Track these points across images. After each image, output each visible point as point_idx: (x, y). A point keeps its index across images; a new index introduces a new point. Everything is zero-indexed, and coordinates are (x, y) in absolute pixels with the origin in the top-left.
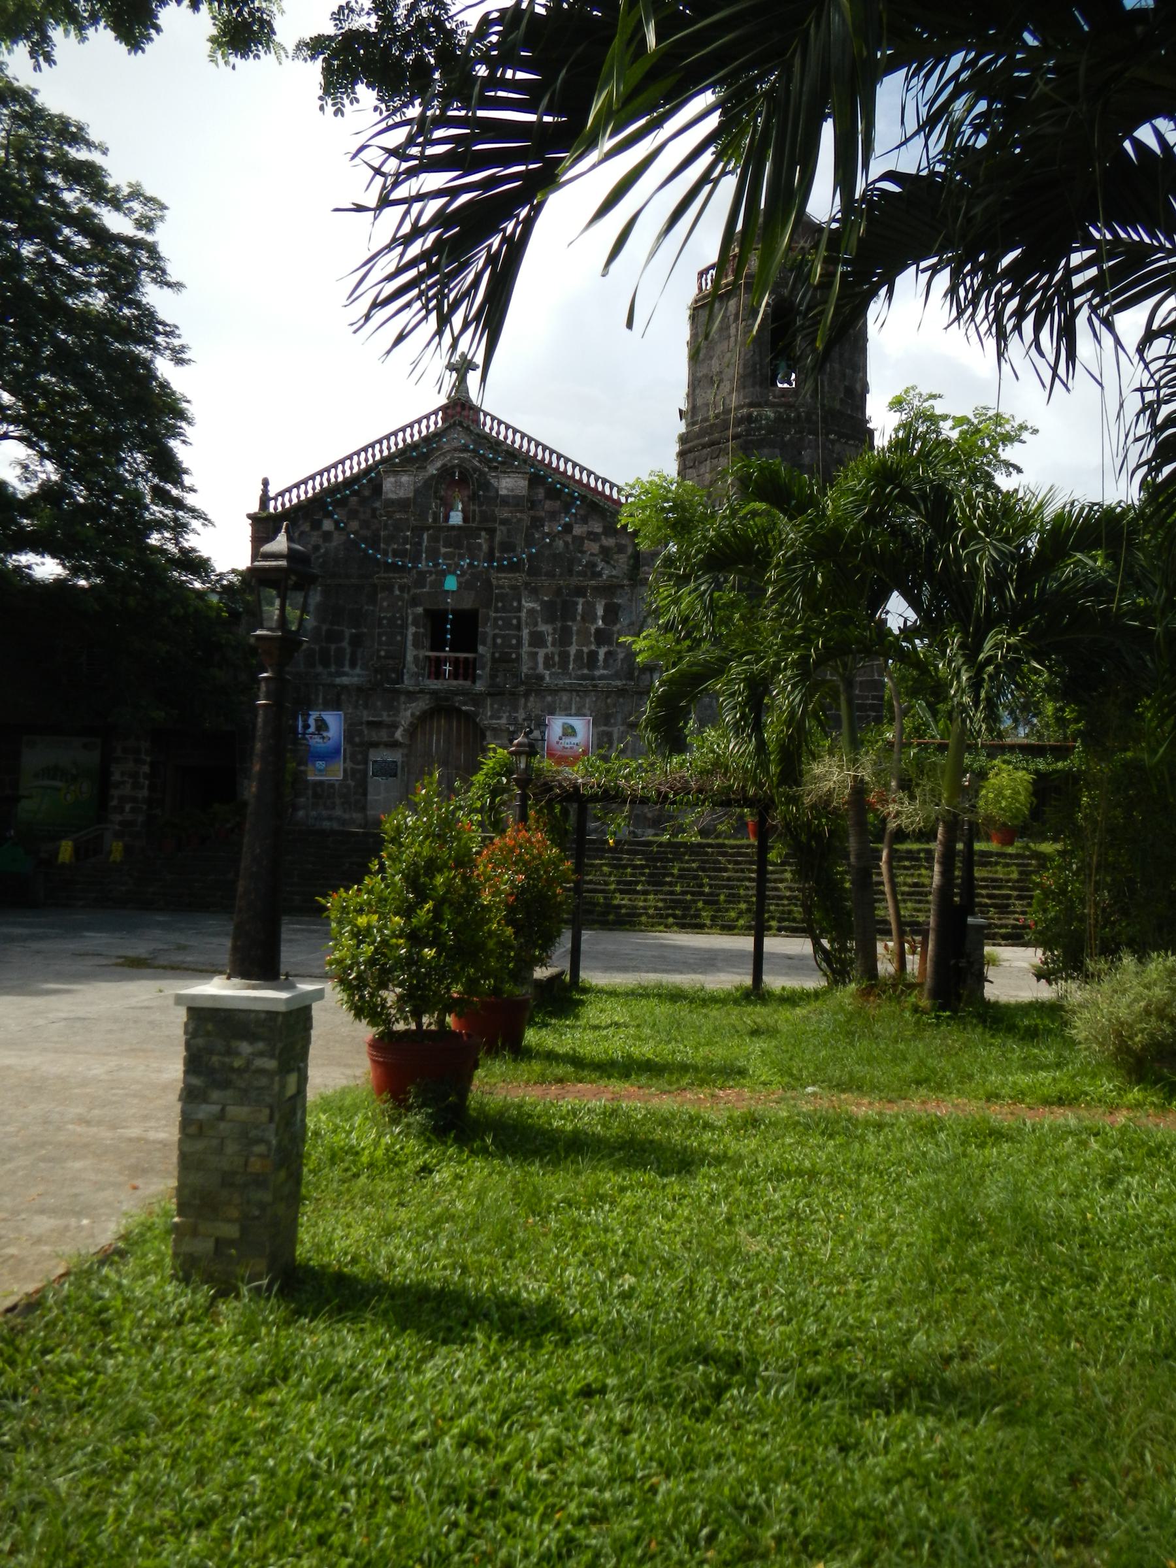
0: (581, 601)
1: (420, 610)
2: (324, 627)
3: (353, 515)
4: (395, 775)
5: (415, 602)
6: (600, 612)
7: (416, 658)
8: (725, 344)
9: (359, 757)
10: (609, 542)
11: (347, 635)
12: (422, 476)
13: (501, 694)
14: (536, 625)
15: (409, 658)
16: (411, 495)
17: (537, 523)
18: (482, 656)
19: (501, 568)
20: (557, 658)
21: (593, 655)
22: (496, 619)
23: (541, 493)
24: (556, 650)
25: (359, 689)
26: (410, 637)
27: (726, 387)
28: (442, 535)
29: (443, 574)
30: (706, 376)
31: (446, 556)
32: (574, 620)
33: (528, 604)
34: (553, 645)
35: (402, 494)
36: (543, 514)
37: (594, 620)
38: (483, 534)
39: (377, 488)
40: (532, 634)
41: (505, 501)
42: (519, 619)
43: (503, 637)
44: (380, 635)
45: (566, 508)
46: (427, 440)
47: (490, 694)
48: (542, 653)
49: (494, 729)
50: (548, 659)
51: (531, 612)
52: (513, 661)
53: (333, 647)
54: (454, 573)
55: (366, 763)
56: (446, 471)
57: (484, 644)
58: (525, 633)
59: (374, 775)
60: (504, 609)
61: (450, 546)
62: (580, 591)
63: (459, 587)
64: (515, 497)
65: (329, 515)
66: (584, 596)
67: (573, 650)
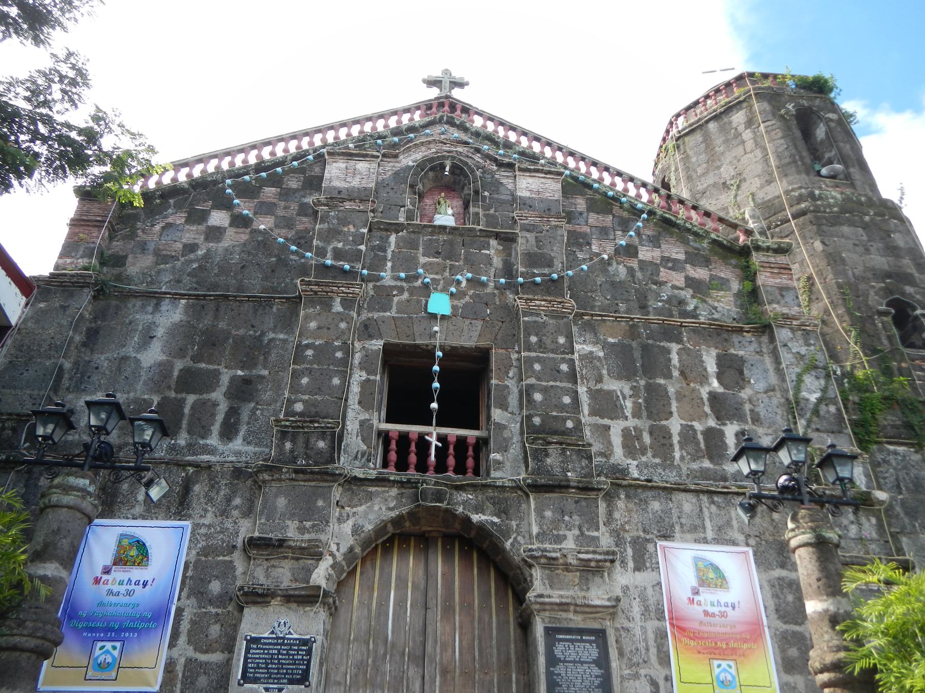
0: (675, 347)
1: (377, 345)
2: (179, 365)
3: (266, 209)
4: (304, 679)
5: (368, 330)
6: (711, 367)
7: (362, 423)
8: (741, 148)
9: (215, 630)
10: (701, 273)
11: (225, 379)
12: (391, 167)
13: (561, 487)
14: (600, 380)
15: (352, 426)
16: (373, 185)
17: (577, 240)
18: (501, 427)
19: (531, 286)
20: (647, 439)
21: (714, 438)
22: (530, 362)
23: (580, 204)
24: (644, 424)
25: (238, 473)
26: (355, 389)
27: (753, 184)
28: (423, 239)
29: (426, 290)
30: (715, 185)
31: (427, 267)
32: (669, 376)
33: (582, 347)
34: (636, 414)
35: (355, 183)
36: (587, 229)
37: (704, 378)
38: (493, 242)
39: (314, 183)
40: (595, 395)
41: (525, 204)
42: (571, 363)
43: (545, 390)
44: (296, 375)
45: (625, 225)
46: (397, 132)
47: (537, 488)
48: (616, 428)
49: (550, 564)
50: (631, 440)
51: (589, 358)
52: (566, 432)
53: (191, 399)
54: (444, 290)
55: (230, 648)
56: (433, 166)
57: (504, 406)
58: (582, 390)
59: (245, 678)
60: (541, 346)
61: (437, 254)
62: (671, 333)
63: (454, 314)
64: (542, 201)
65: (225, 204)
66: (679, 341)
67: (675, 425)
